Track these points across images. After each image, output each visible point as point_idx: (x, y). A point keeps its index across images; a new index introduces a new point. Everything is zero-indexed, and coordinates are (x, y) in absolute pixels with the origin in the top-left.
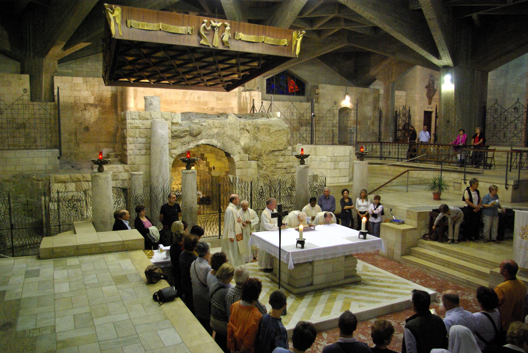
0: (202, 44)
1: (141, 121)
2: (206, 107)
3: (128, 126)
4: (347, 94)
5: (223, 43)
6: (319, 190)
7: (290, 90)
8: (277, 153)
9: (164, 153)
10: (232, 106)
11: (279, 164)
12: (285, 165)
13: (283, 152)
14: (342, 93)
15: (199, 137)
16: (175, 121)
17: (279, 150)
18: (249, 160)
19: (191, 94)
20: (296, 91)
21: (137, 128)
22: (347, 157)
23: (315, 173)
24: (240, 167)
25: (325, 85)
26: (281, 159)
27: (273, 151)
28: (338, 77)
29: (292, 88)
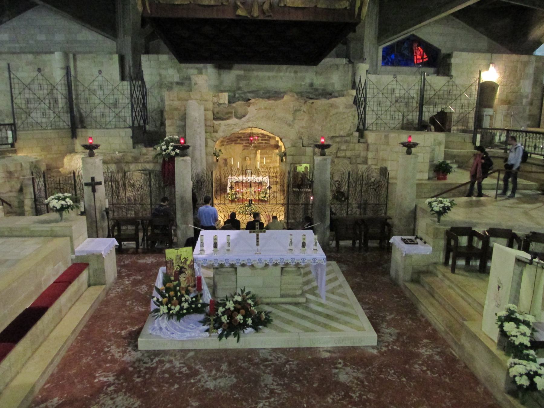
0: (239, 16)
1: (180, 102)
2: (303, 83)
3: (167, 108)
4: (492, 63)
5: (263, 12)
6: (379, 186)
7: (415, 61)
8: (338, 140)
9: (198, 136)
10: (334, 81)
11: (341, 152)
12: (349, 154)
13: (348, 138)
14: (484, 63)
15: (244, 119)
16: (221, 101)
17: (342, 136)
18: (303, 146)
19: (287, 69)
20: (424, 60)
21: (176, 109)
22: (427, 148)
23: (384, 165)
24: (291, 153)
25: (459, 53)
26: (344, 147)
27: (333, 137)
28: (484, 41)
29: (419, 57)
